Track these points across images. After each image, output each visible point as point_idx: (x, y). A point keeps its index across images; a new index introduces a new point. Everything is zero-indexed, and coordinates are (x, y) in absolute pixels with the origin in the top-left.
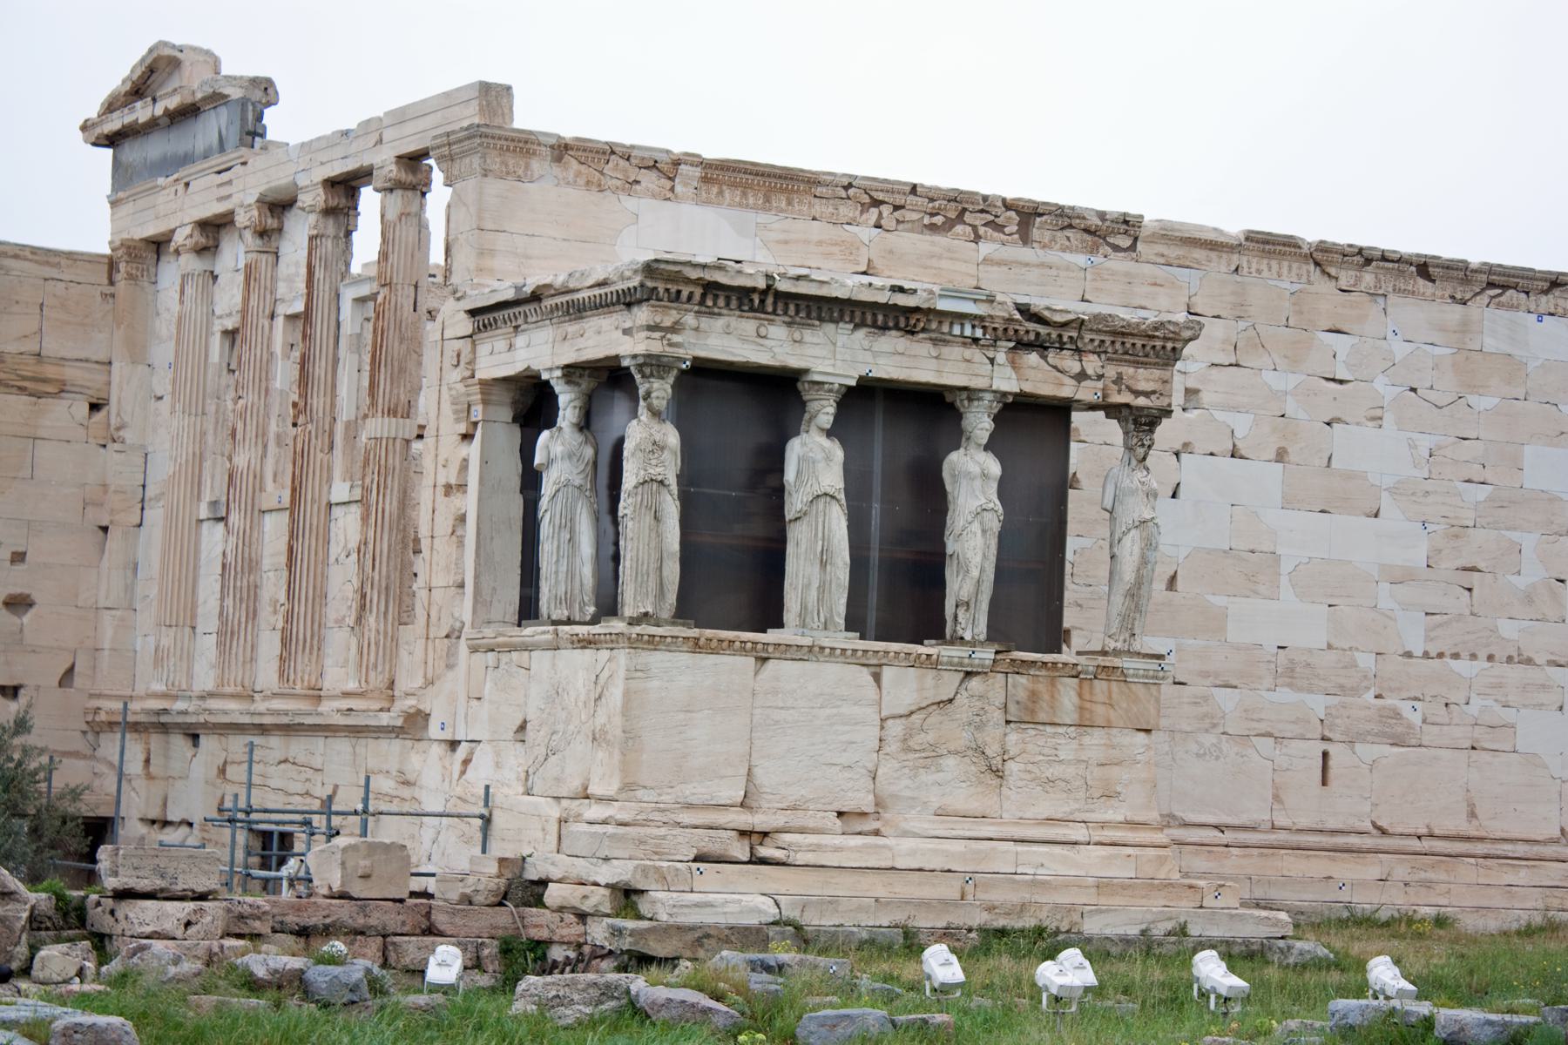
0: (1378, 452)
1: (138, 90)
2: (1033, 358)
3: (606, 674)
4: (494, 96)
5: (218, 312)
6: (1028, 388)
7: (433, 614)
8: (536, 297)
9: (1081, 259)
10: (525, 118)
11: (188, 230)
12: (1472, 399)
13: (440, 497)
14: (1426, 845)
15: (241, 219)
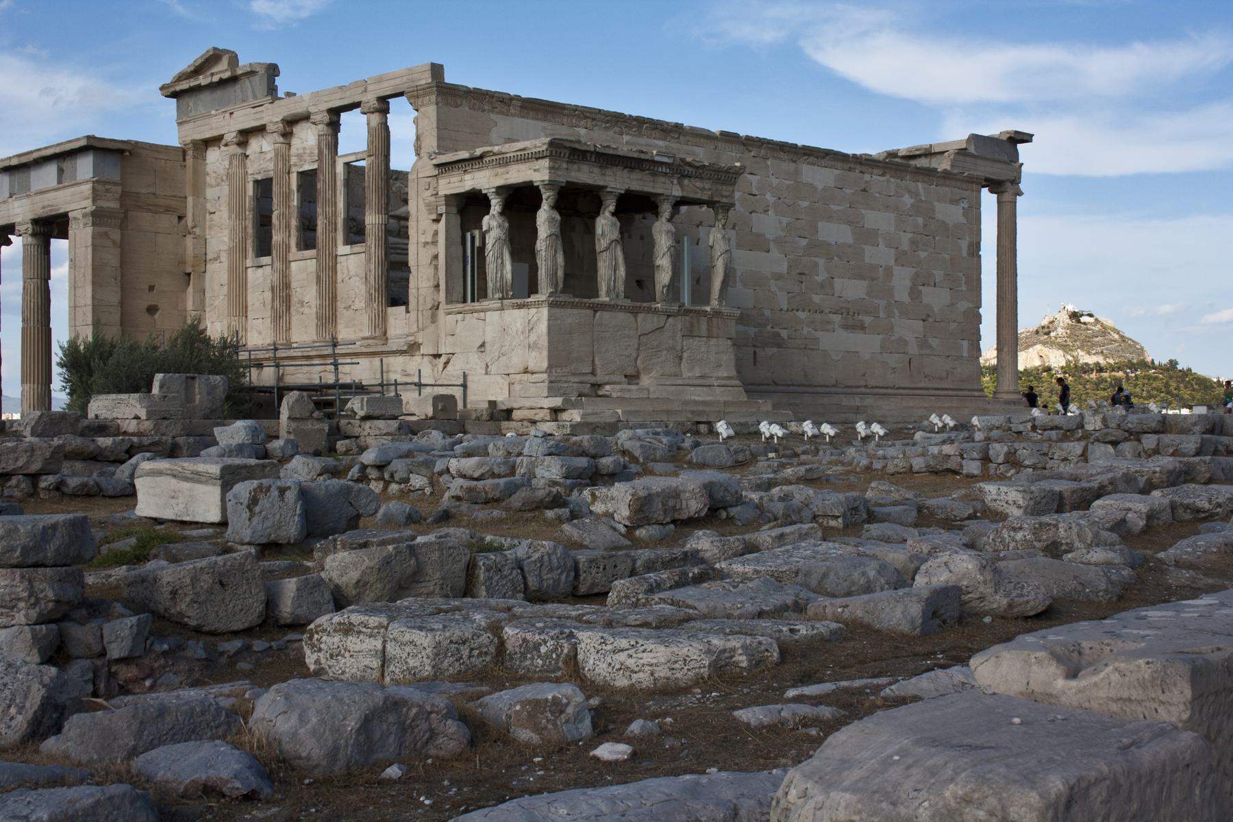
0: (769, 224)
1: (198, 70)
2: (686, 181)
3: (535, 318)
4: (437, 70)
5: (250, 171)
6: (685, 194)
7: (421, 299)
8: (481, 157)
9: (661, 143)
10: (449, 78)
11: (234, 134)
12: (801, 203)
13: (421, 249)
14: (792, 388)
15: (270, 128)
